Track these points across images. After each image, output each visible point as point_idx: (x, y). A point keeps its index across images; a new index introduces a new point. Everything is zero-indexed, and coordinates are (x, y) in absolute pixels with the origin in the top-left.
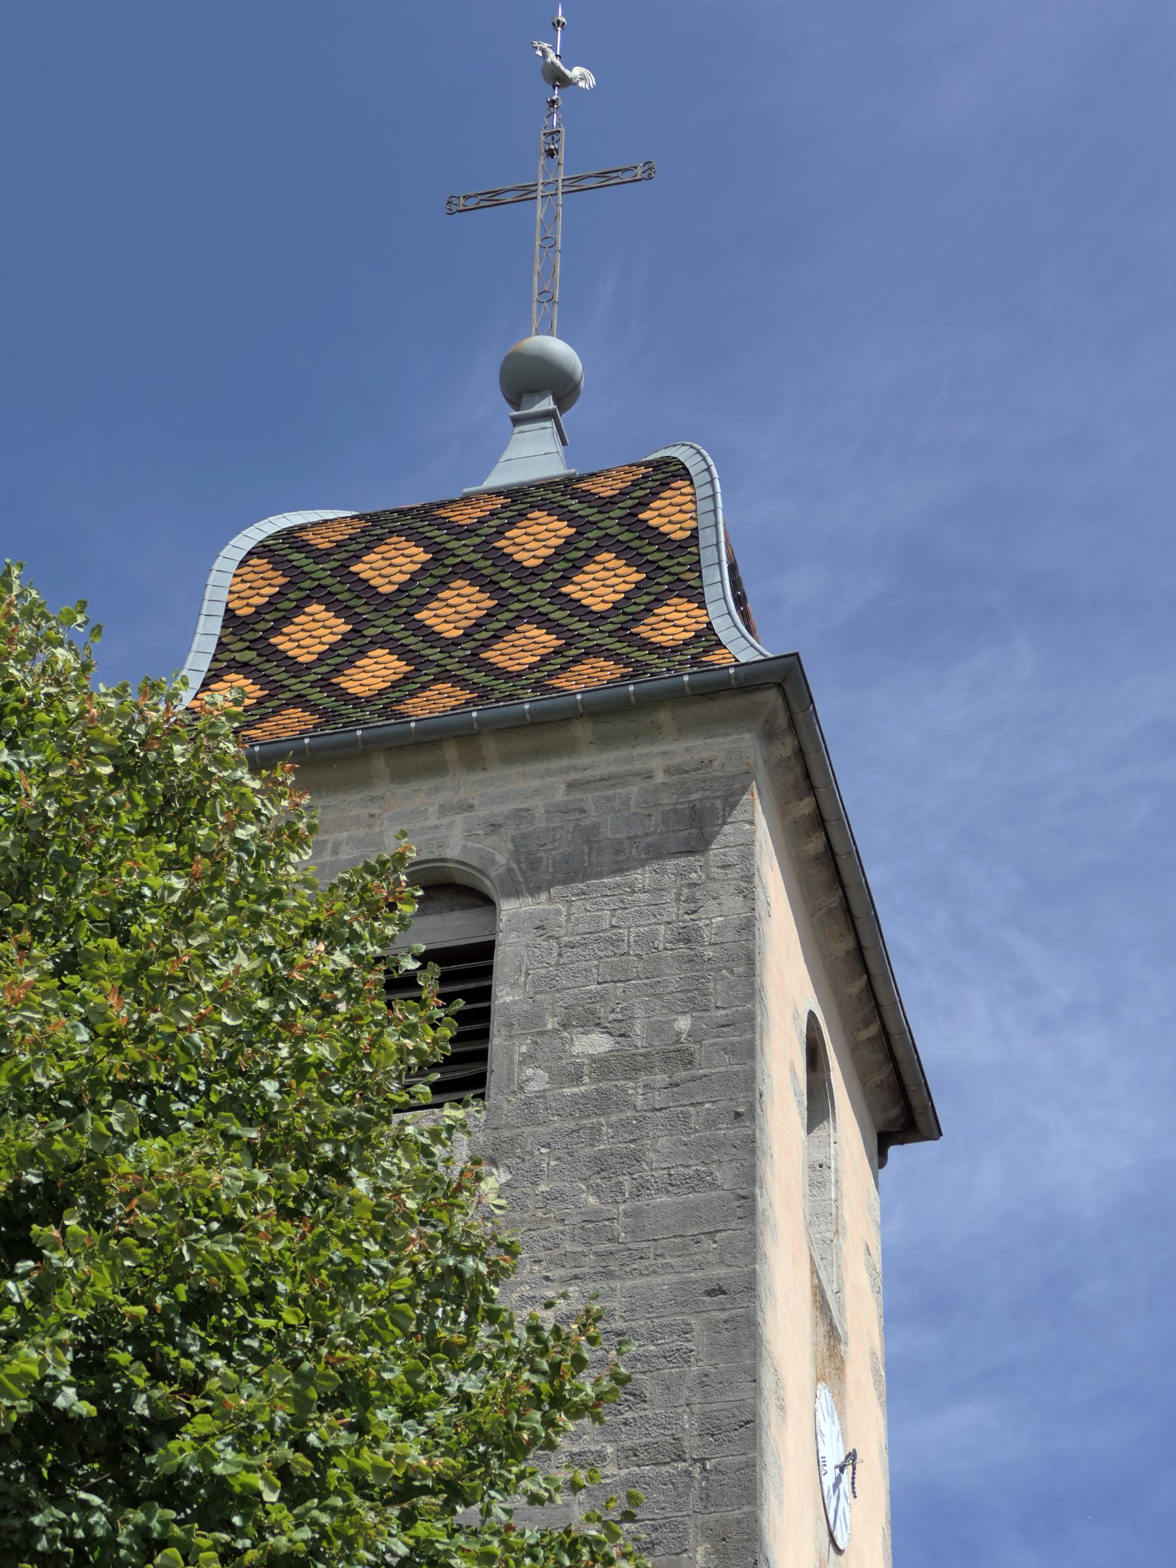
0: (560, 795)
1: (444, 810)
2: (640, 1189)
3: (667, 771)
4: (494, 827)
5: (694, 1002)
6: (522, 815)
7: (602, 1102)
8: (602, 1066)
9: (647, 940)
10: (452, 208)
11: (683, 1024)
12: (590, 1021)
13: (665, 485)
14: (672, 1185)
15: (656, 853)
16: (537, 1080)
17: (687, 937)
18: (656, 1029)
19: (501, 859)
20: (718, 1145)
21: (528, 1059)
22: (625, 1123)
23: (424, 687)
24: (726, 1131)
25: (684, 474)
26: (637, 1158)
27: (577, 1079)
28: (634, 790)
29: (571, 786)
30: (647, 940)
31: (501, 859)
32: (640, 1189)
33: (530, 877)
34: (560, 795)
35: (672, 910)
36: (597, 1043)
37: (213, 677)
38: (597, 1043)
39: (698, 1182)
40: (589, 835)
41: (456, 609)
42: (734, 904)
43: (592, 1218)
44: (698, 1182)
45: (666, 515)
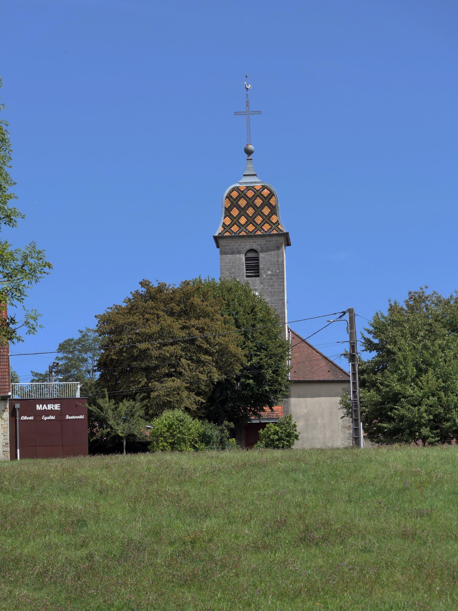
0: (265, 242)
1: (253, 242)
2: (275, 289)
3: (275, 241)
4: (258, 245)
5: (279, 269)
6: (261, 244)
7: (271, 279)
8: (271, 275)
9: (274, 261)
10: (236, 113)
11: (278, 271)
12: (268, 269)
13: (272, 197)
14: (277, 288)
15: (274, 250)
16: (265, 276)
17: (278, 261)
18: (275, 272)
19: (259, 249)
20: (281, 285)
21: (264, 273)
22: (273, 282)
23: (249, 225)
24: (282, 283)
25: (273, 195)
26: (274, 285)
27: (268, 276)
28: (272, 243)
29: (266, 241)
30: (274, 261)
31: (259, 249)
32: (275, 289)
33: (262, 251)
34: (265, 242)
35: (276, 258)
36: (269, 272)
37: (225, 217)
38: (269, 272)
39: (280, 288)
40: (268, 247)
41: (250, 211)
42: (282, 258)
43: (270, 291)
44: (280, 288)
45: (272, 201)
